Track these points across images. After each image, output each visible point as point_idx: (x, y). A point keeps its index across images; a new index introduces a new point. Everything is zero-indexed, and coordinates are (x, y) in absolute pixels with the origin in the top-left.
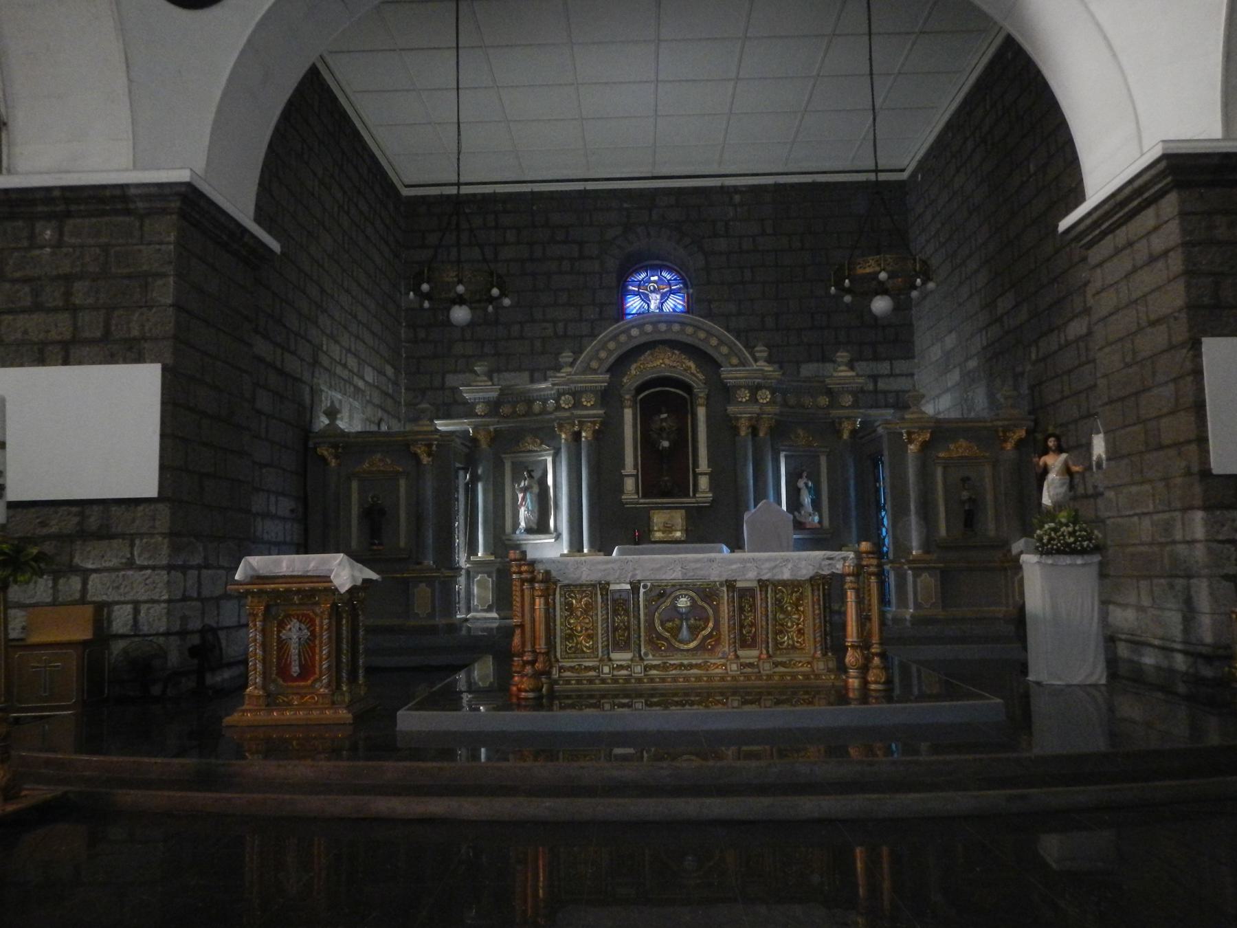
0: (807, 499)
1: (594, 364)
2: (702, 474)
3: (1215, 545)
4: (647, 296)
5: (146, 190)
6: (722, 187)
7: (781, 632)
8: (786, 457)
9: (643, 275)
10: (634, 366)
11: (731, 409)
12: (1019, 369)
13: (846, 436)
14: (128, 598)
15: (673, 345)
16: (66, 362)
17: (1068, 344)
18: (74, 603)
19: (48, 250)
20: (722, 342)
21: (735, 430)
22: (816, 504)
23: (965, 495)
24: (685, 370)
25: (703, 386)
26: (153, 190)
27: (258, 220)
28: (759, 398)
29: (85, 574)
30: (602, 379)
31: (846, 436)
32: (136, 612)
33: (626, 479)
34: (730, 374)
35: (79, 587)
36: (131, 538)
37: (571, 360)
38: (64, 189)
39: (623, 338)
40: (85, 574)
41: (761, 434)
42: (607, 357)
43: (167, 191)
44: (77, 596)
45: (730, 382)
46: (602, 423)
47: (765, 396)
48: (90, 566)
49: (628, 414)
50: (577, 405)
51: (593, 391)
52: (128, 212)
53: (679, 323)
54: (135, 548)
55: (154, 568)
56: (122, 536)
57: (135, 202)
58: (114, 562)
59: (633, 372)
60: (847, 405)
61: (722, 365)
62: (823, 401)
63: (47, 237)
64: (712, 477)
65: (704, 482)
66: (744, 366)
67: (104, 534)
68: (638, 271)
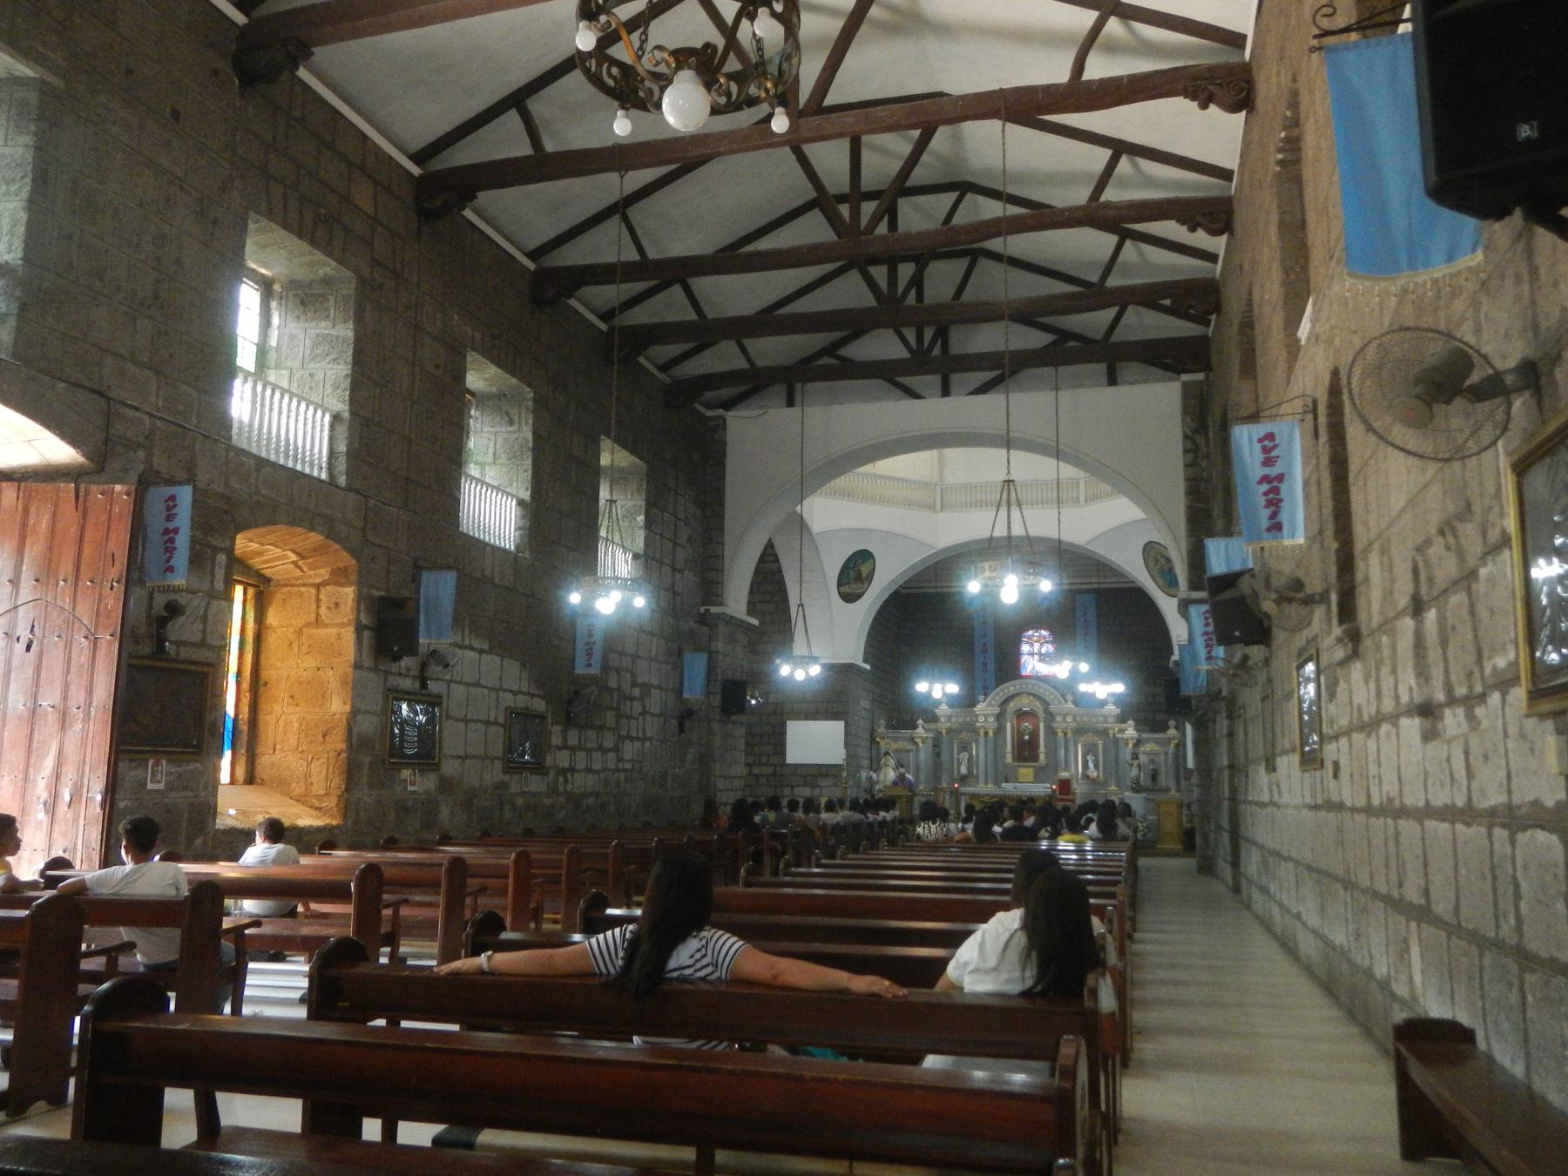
0: (1091, 765)
4: (1032, 645)
9: (1030, 632)
11: (1054, 725)
21: (1056, 734)
22: (1096, 767)
23: (1151, 767)
27: (865, 661)
30: (997, 710)
40: (820, 787)
41: (1069, 735)
47: (1069, 719)
49: (1009, 725)
50: (986, 720)
51: (993, 715)
65: (1042, 756)
67: (826, 775)
68: (1028, 630)
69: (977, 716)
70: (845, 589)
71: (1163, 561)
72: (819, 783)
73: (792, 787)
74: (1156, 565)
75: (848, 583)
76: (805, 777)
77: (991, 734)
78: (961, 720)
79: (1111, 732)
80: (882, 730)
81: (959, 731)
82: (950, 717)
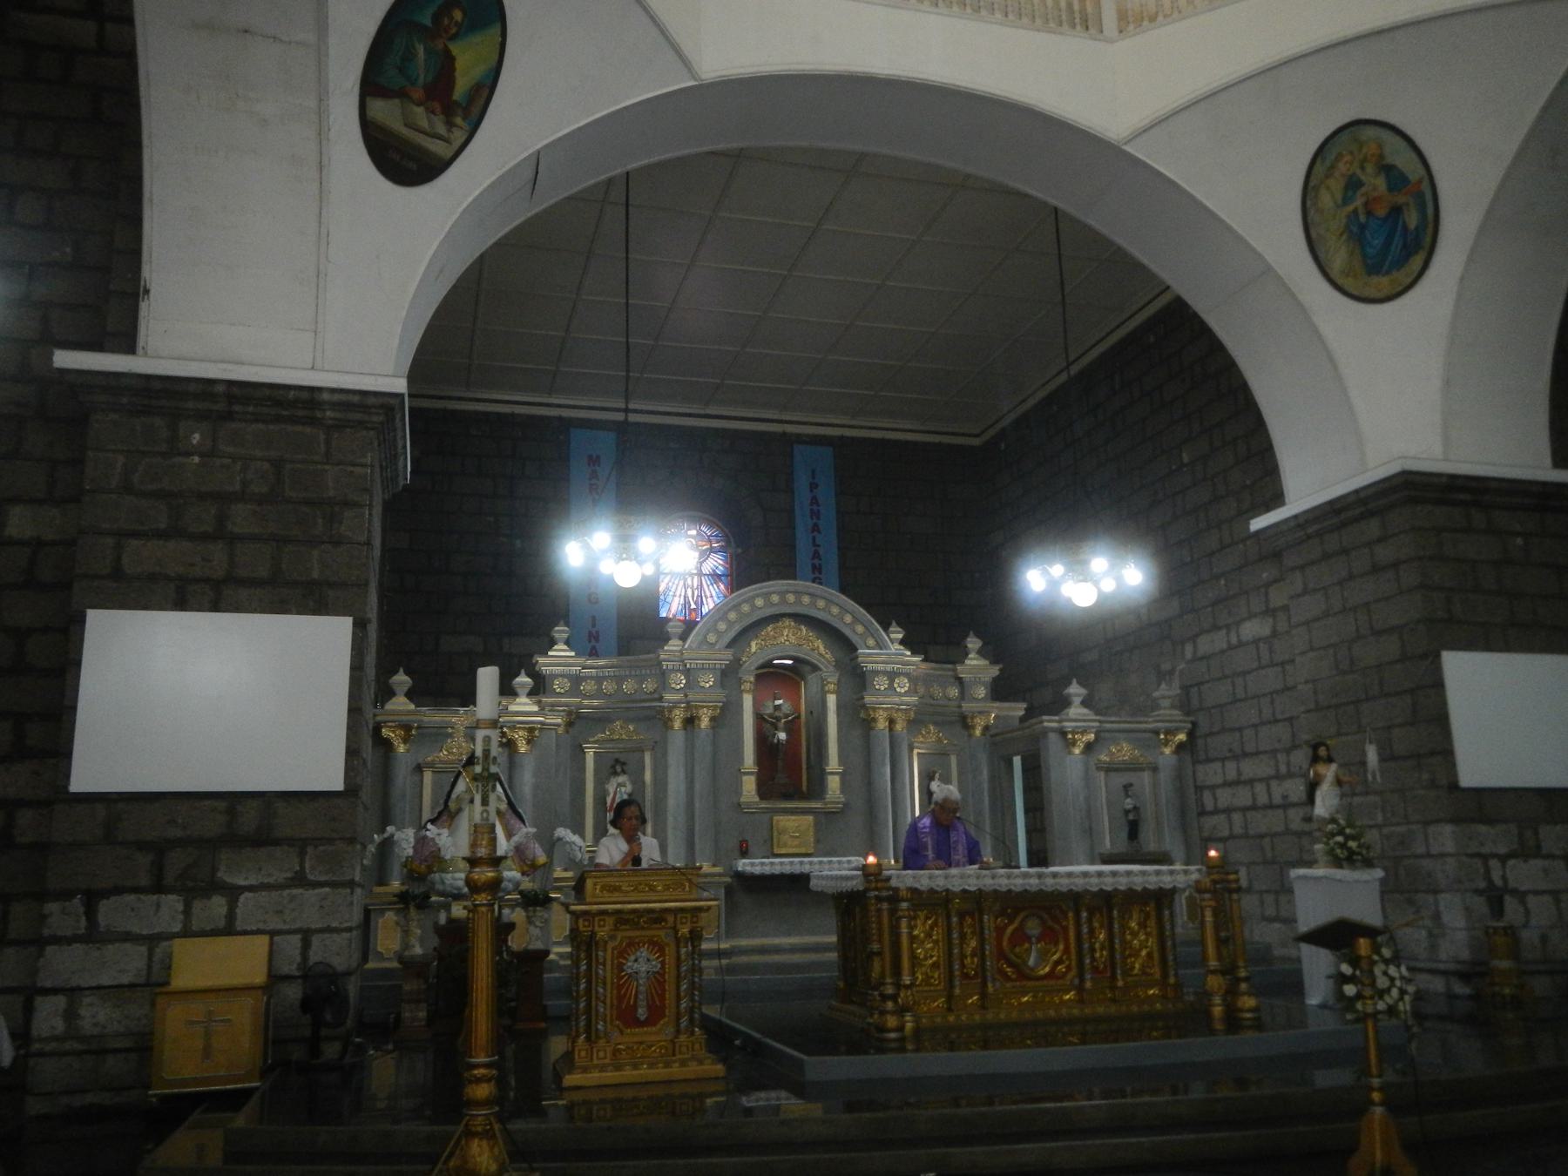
1: (712, 638)
2: (832, 773)
3: (1464, 859)
5: (343, 397)
6: (784, 434)
7: (1130, 956)
8: (919, 754)
10: (753, 644)
12: (1166, 666)
13: (978, 732)
14: (298, 925)
15: (801, 618)
16: (215, 608)
17: (1241, 644)
18: (215, 933)
19: (196, 459)
20: (856, 620)
21: (868, 724)
23: (1129, 803)
24: (813, 650)
25: (832, 669)
26: (356, 399)
28: (896, 685)
29: (233, 893)
31: (978, 732)
32: (306, 945)
33: (745, 778)
34: (869, 656)
35: (224, 910)
36: (301, 845)
37: (680, 631)
38: (231, 383)
39: (746, 608)
40: (233, 893)
41: (899, 727)
42: (726, 630)
43: (371, 401)
44: (222, 924)
45: (866, 667)
46: (722, 709)
48: (242, 883)
49: (748, 700)
51: (712, 670)
52: (312, 421)
53: (809, 594)
54: (307, 858)
55: (333, 885)
56: (291, 841)
57: (324, 410)
58: (279, 876)
59: (754, 648)
60: (980, 697)
61: (858, 646)
62: (954, 692)
63: (195, 442)
64: (843, 775)
65: (834, 783)
66: (881, 649)
67: (263, 839)
69: (663, 676)
70: (385, 111)
71: (1381, 183)
72: (223, 875)
73: (92, 899)
74: (1346, 201)
75: (402, 94)
76: (159, 849)
77: (705, 723)
78: (608, 687)
79: (979, 724)
80: (400, 704)
81: (600, 720)
82: (576, 680)
